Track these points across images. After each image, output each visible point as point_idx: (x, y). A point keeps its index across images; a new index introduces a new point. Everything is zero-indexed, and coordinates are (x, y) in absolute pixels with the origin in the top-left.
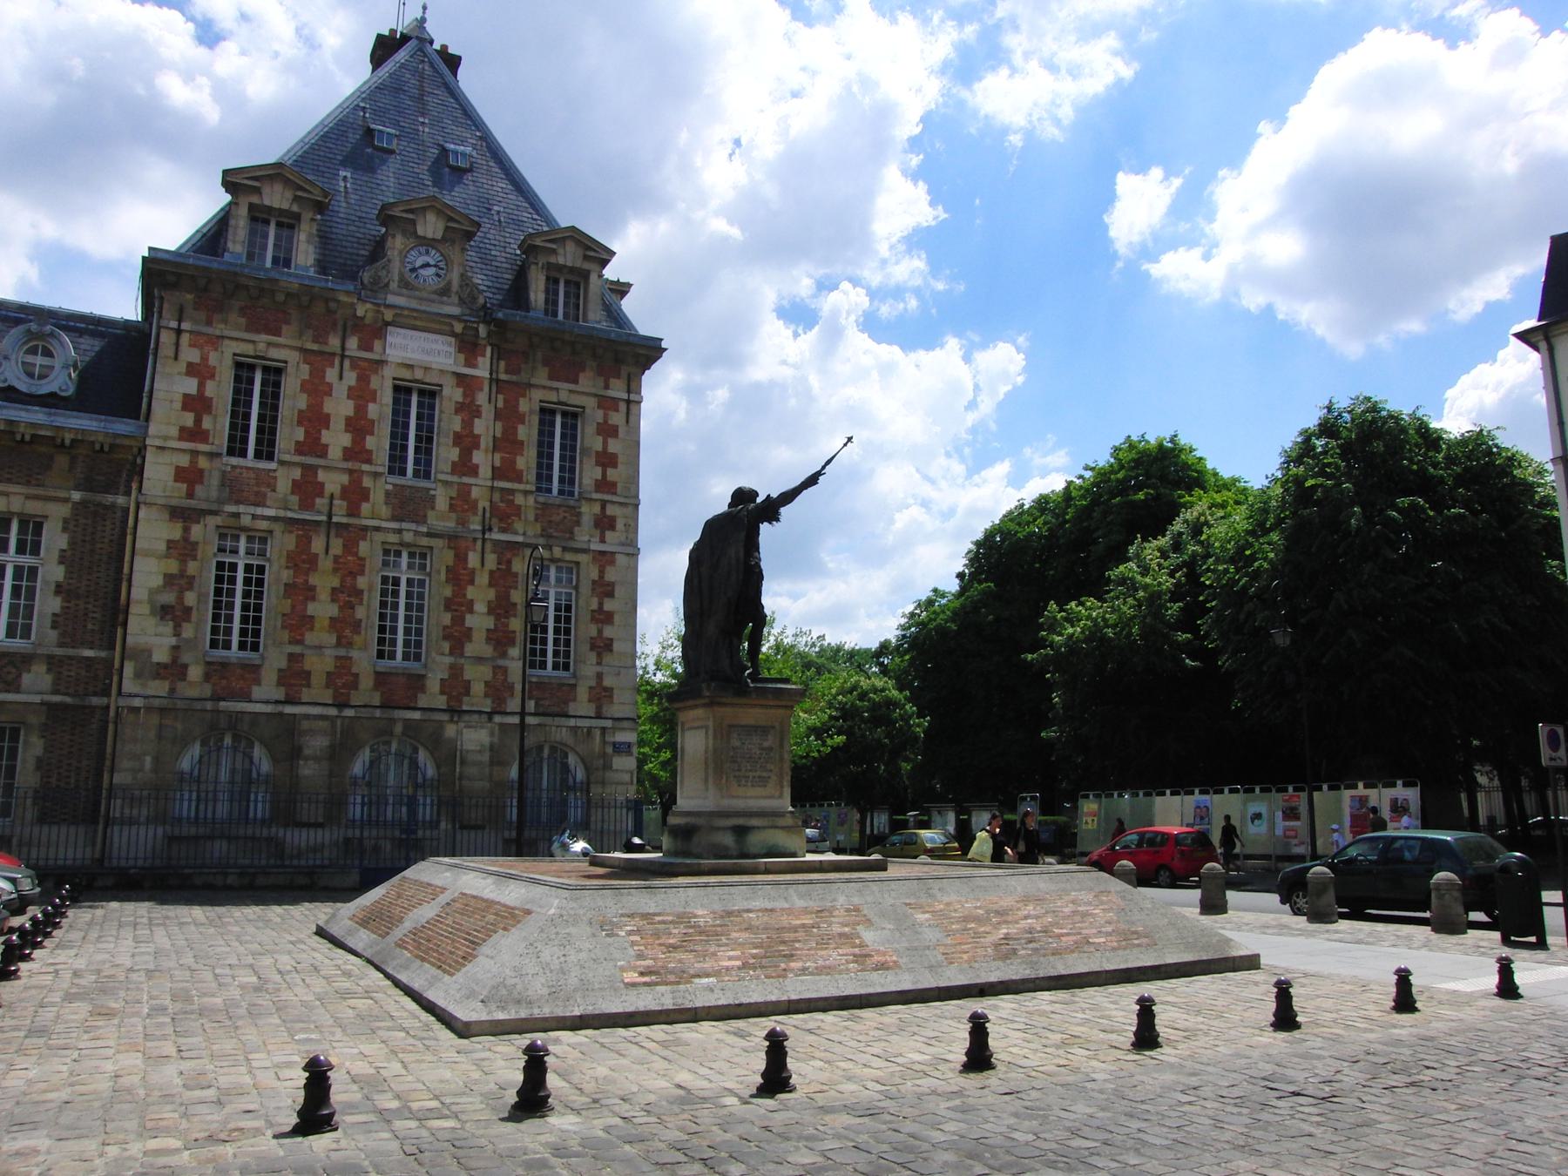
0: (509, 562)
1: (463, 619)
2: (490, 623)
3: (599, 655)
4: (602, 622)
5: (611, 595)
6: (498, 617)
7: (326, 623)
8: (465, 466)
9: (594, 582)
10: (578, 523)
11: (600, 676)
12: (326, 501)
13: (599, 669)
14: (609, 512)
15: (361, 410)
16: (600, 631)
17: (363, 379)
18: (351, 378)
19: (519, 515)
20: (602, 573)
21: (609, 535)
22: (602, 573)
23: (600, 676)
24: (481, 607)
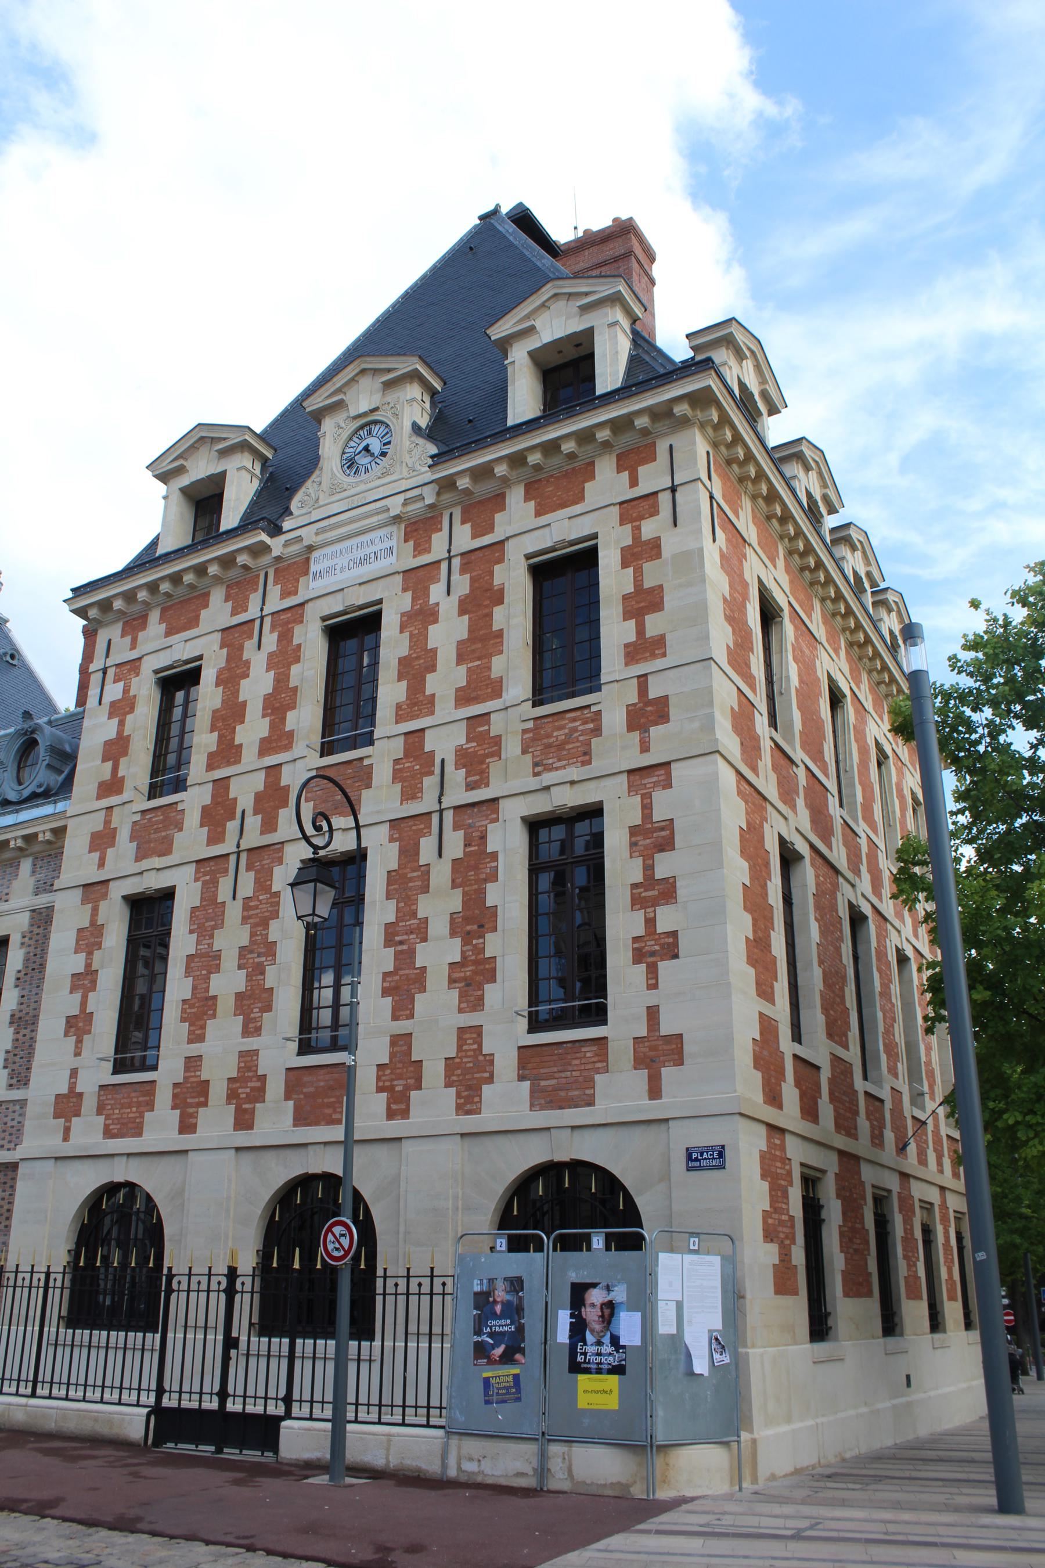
0: (483, 838)
1: (412, 953)
2: (453, 950)
3: (652, 971)
4: (655, 903)
5: (667, 844)
6: (467, 938)
7: (232, 1001)
8: (418, 702)
9: (634, 831)
10: (597, 731)
11: (653, 1014)
12: (237, 822)
13: (651, 998)
14: (653, 693)
15: (281, 682)
16: (650, 923)
17: (285, 637)
18: (271, 641)
19: (498, 754)
20: (647, 808)
21: (656, 732)
22: (647, 808)
23: (653, 1014)
24: (439, 927)
